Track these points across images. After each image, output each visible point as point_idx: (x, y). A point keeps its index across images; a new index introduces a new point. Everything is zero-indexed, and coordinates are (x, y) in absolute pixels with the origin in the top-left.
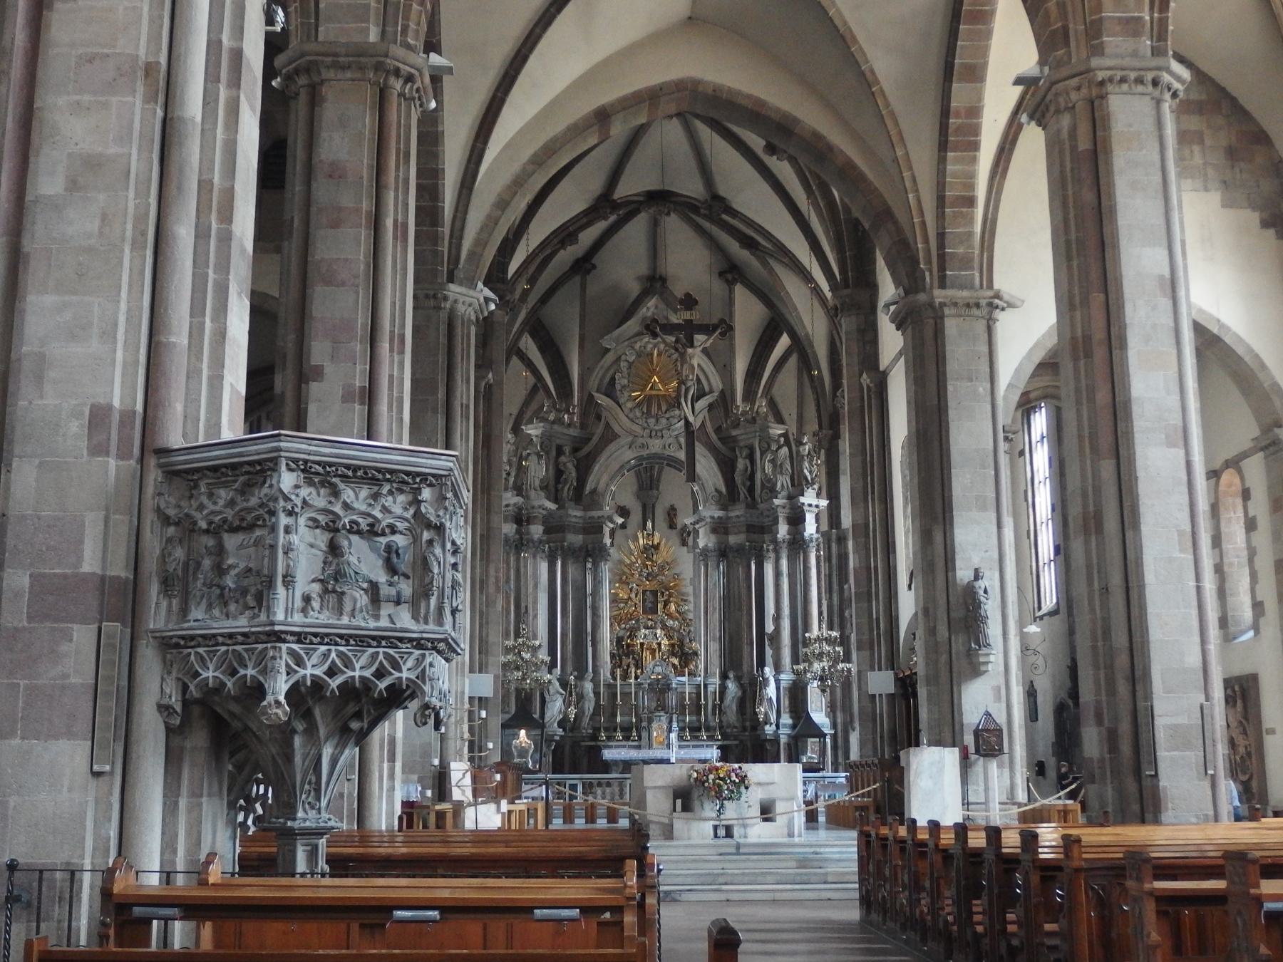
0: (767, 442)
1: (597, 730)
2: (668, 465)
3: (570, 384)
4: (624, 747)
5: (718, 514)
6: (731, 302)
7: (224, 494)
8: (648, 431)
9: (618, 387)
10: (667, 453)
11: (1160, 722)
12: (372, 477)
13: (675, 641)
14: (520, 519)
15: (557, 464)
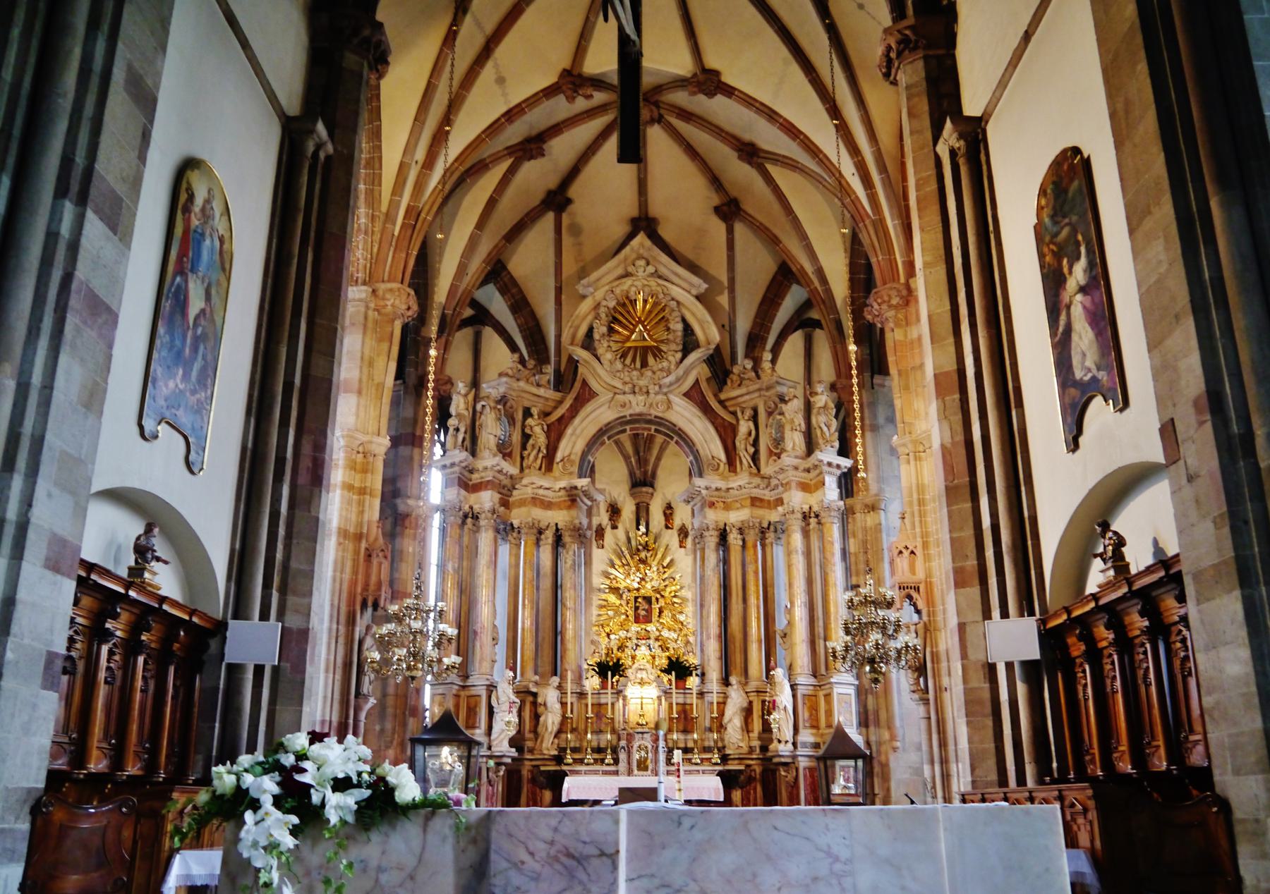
1: (562, 750)
2: (656, 431)
3: (546, 349)
4: (596, 772)
8: (630, 385)
9: (596, 336)
10: (654, 412)
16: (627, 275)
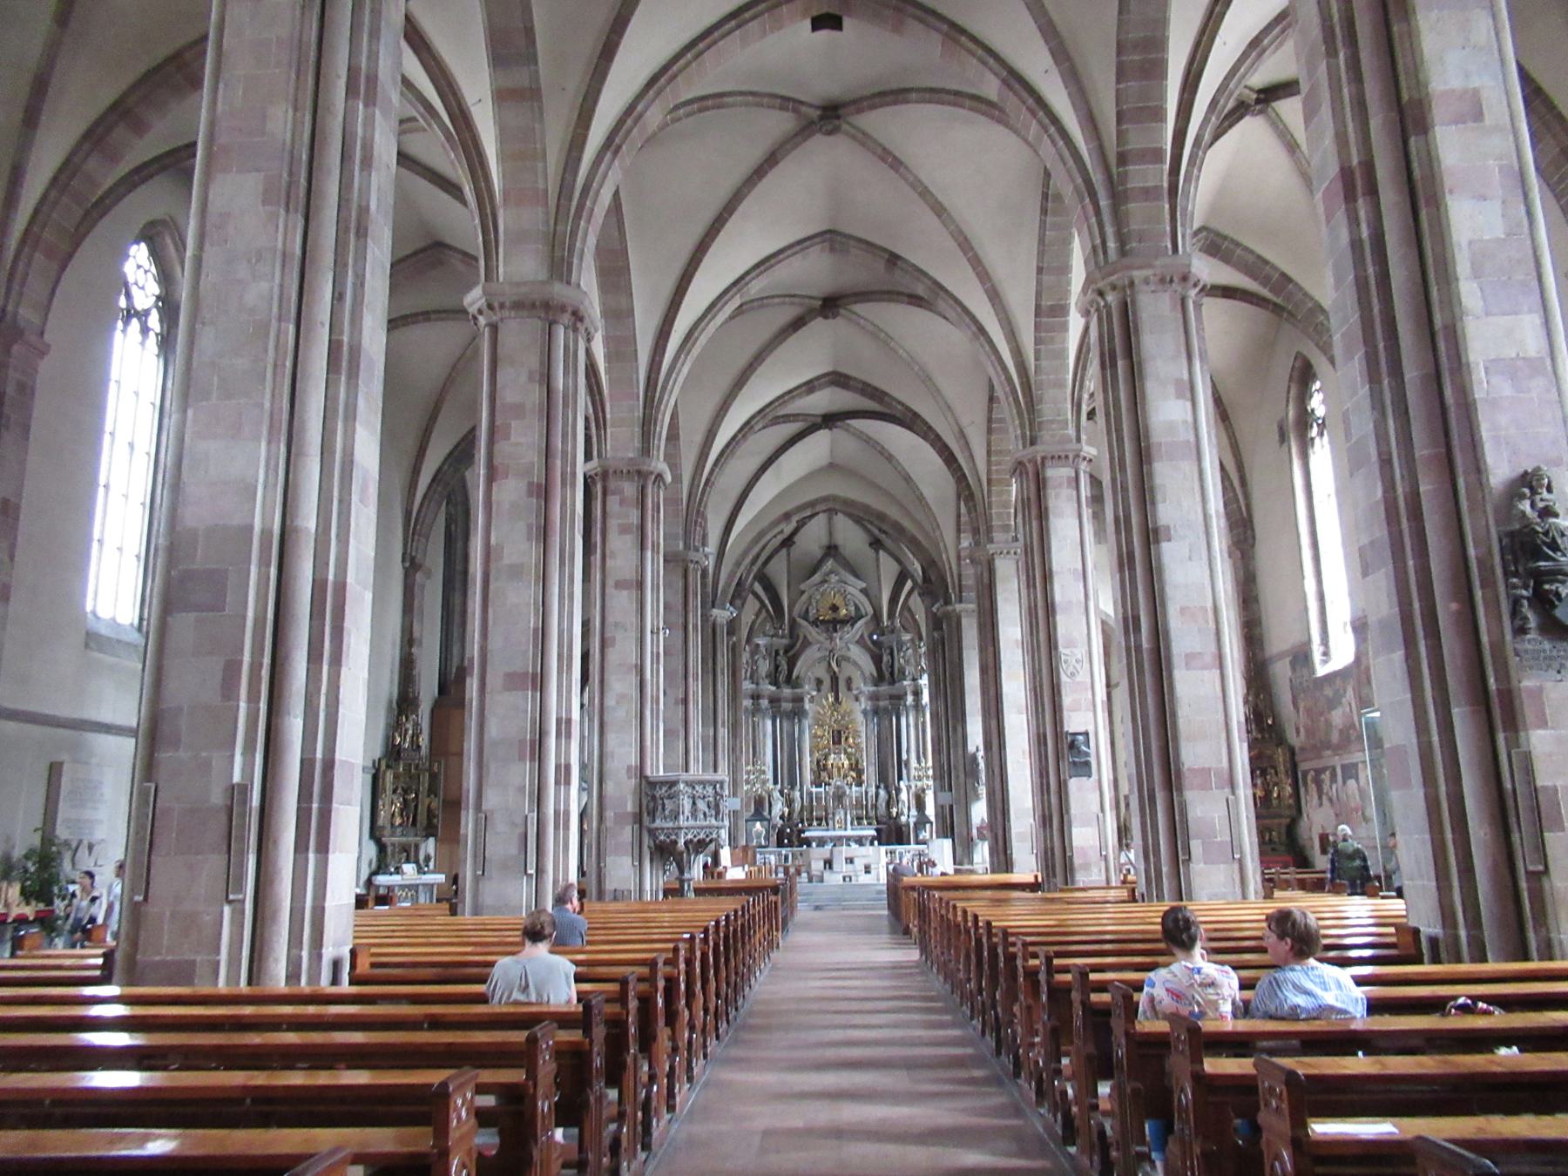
0: (901, 644)
5: (872, 689)
6: (878, 560)
7: (664, 789)
11: (1013, 831)
12: (703, 783)
13: (853, 761)
14: (756, 697)
15: (776, 659)
16: (824, 581)
